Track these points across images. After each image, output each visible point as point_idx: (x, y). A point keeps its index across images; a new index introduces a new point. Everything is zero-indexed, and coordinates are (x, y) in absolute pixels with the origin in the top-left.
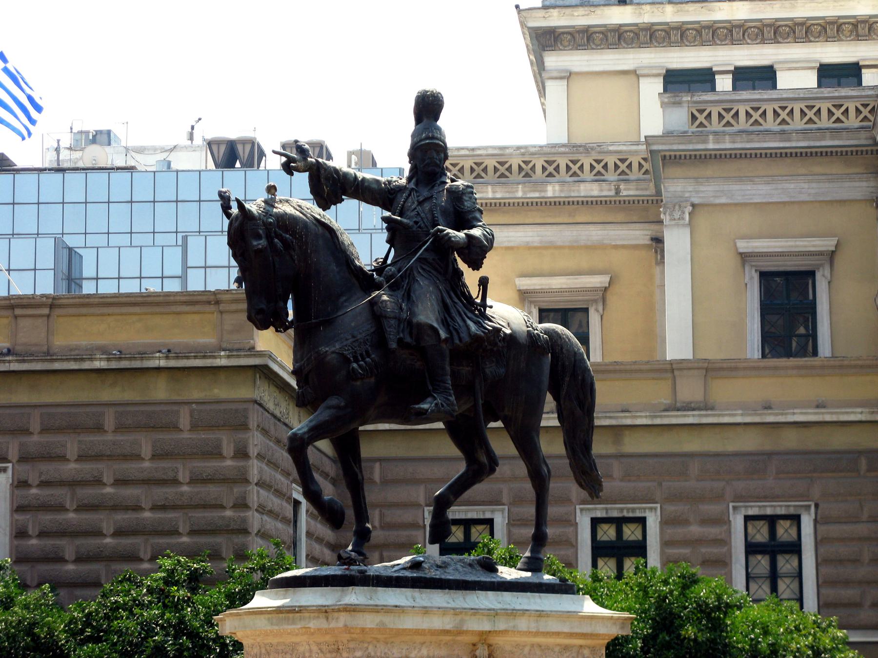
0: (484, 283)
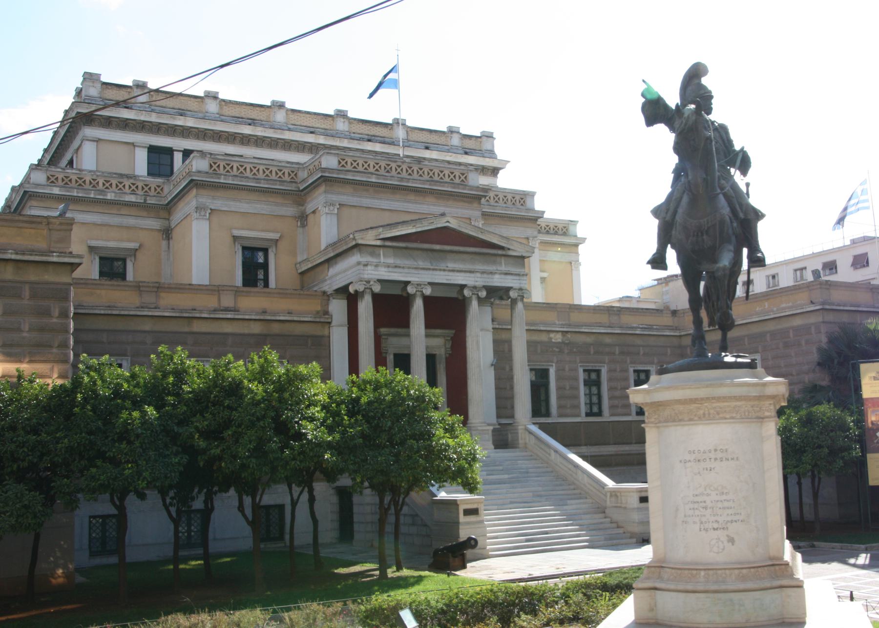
0: (748, 185)
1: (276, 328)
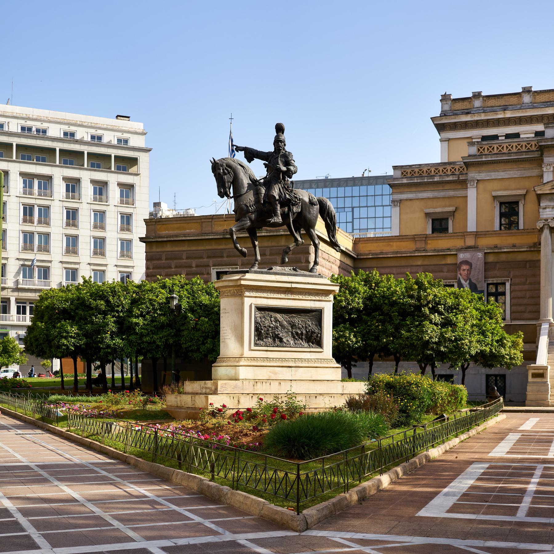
1: (503, 257)
